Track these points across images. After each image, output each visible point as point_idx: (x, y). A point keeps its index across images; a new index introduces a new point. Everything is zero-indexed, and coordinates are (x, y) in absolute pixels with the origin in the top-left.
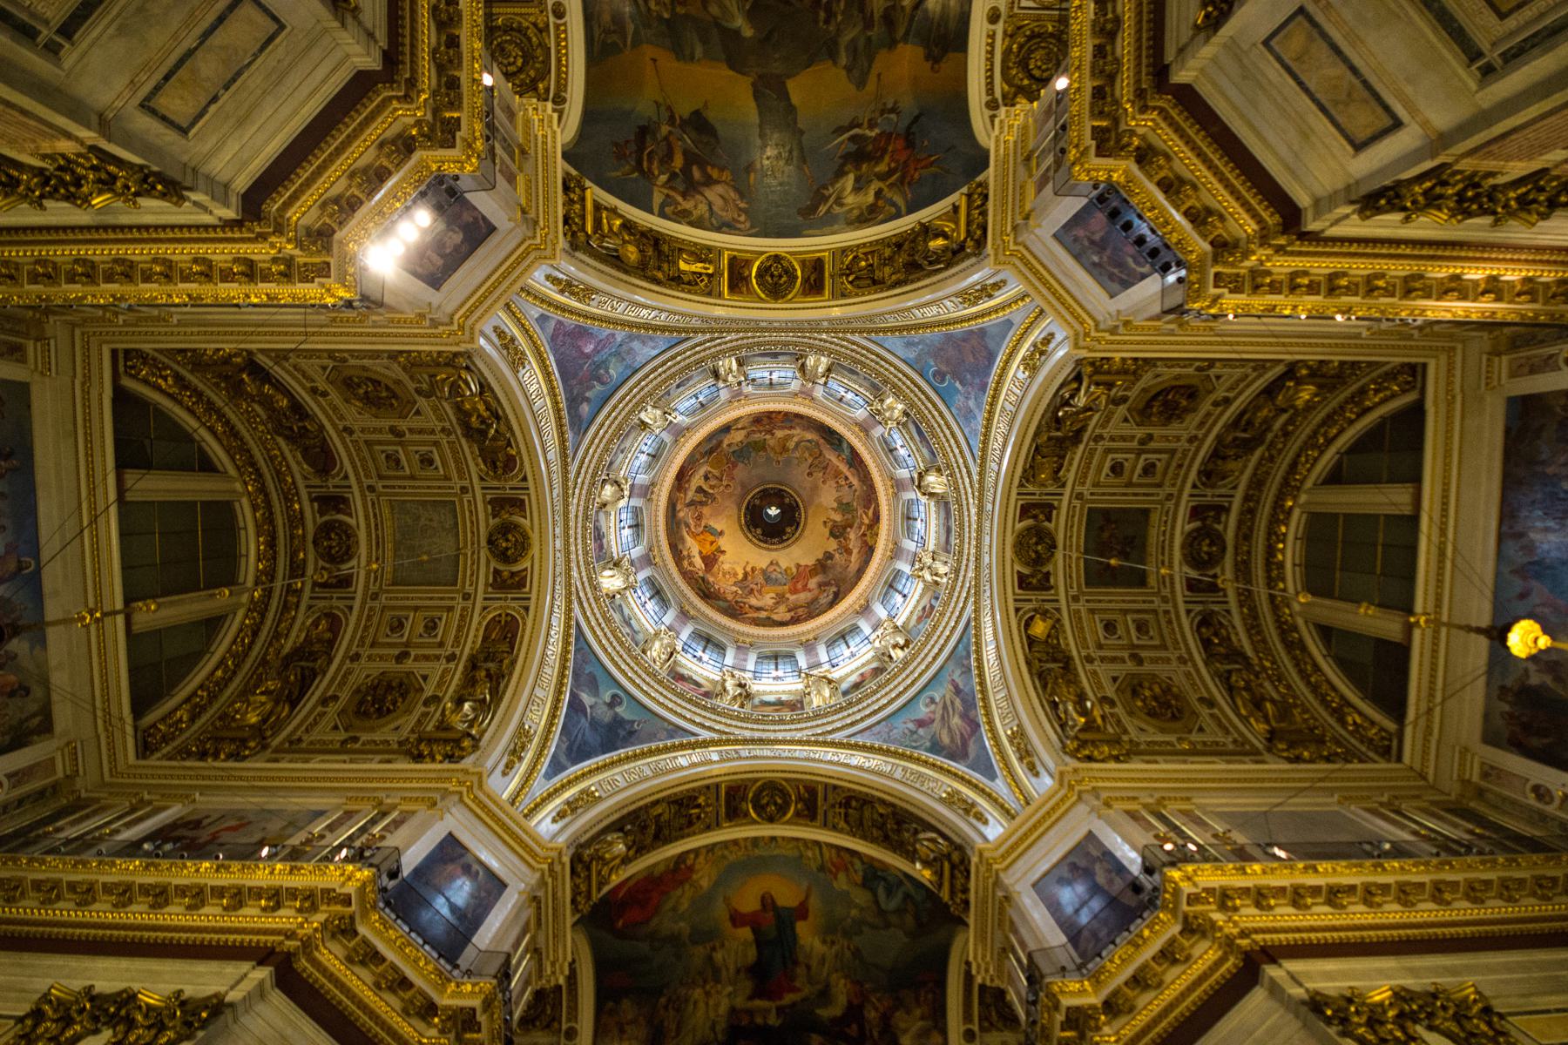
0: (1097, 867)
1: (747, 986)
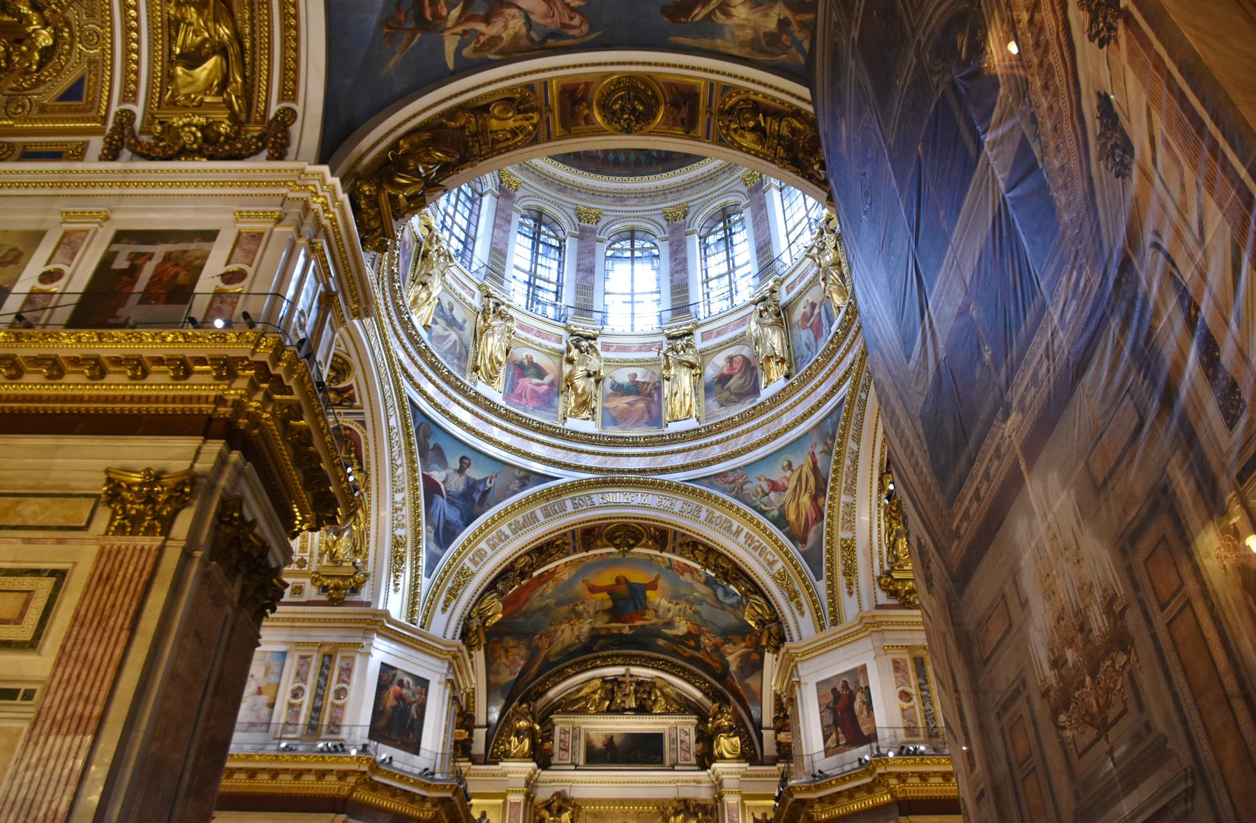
0: (859, 694)
1: (606, 618)
